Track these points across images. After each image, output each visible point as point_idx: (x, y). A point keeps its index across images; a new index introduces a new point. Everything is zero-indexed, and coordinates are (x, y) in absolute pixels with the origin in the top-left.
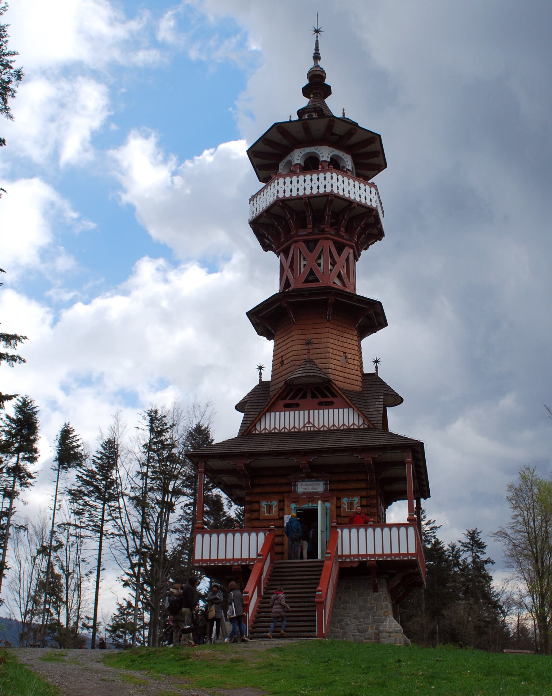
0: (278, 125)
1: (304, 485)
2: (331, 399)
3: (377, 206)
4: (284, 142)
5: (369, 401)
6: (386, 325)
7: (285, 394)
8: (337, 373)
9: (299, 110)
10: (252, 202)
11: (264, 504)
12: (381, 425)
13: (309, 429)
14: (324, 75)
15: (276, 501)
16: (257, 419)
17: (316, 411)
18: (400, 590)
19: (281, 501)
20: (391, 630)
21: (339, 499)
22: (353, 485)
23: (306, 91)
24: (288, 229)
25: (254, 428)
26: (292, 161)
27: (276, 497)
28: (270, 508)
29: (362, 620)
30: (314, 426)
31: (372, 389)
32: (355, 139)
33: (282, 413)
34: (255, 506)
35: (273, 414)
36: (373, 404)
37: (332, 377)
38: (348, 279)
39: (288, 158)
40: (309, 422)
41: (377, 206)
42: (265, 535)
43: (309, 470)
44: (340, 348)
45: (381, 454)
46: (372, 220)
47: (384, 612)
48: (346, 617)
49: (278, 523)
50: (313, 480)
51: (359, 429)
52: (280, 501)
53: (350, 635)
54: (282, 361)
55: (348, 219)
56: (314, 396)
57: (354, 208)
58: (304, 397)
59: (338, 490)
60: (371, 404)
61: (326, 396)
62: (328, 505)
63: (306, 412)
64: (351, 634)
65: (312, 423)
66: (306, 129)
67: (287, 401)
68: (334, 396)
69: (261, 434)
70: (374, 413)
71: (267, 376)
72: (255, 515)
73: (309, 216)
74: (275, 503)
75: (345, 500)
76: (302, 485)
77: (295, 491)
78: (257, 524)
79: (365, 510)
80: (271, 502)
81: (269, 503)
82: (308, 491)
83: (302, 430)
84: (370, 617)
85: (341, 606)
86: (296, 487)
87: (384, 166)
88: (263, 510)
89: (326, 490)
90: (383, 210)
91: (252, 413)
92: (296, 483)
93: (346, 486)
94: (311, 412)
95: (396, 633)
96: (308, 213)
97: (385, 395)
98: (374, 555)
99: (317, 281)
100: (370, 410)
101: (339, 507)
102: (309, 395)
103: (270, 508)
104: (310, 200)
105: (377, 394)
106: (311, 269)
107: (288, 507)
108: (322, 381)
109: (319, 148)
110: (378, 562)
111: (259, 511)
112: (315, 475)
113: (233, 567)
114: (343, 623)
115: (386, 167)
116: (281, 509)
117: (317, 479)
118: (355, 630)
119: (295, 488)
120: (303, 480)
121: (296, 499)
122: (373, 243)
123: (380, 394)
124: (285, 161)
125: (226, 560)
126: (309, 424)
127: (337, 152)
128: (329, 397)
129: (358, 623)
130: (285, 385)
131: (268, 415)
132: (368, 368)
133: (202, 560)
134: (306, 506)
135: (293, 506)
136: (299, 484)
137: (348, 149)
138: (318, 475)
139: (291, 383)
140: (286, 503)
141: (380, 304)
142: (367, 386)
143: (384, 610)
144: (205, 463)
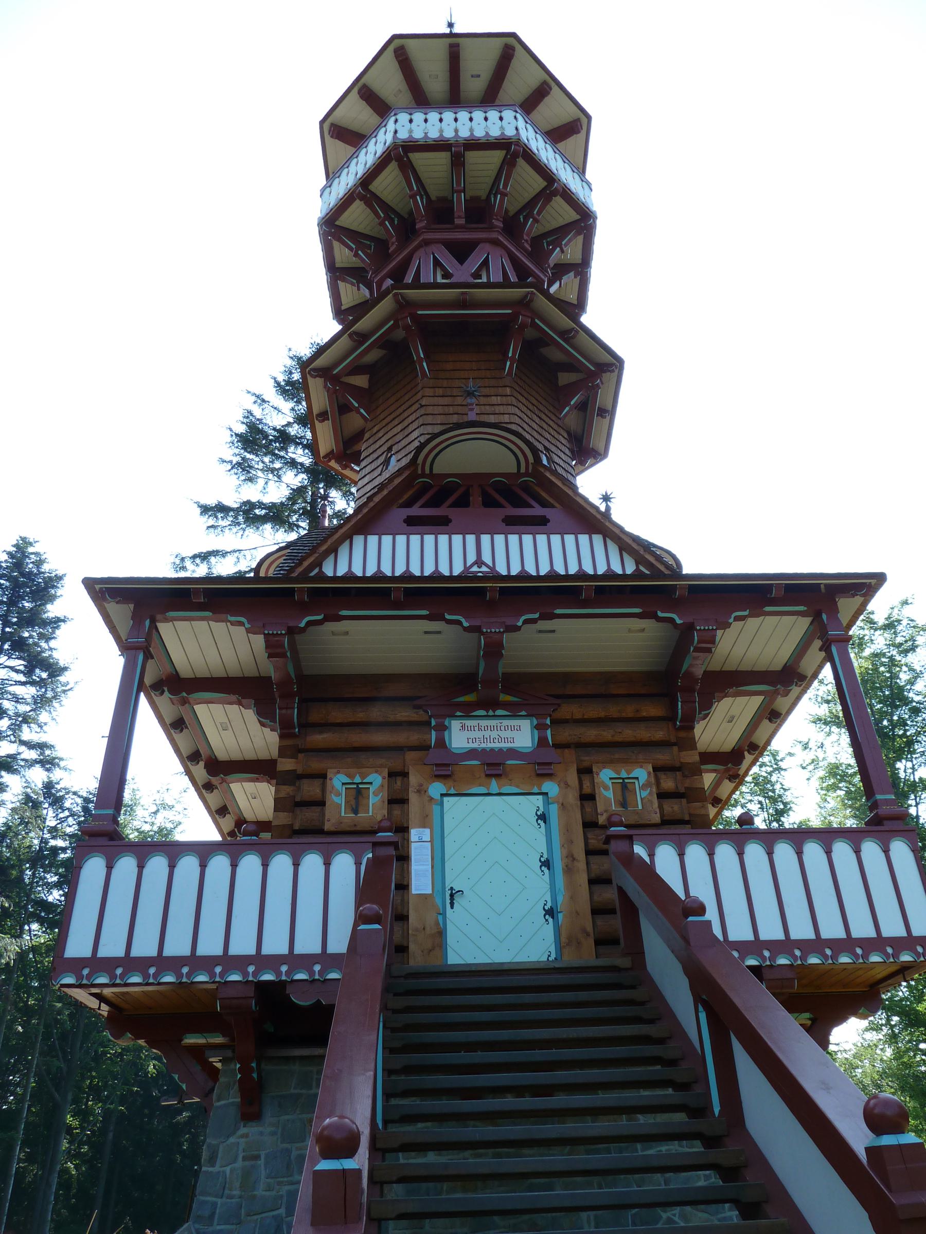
1: (470, 729)
11: (338, 781)
19: (397, 775)
21: (585, 771)
28: (358, 795)
33: (401, 539)
34: (310, 789)
35: (373, 540)
42: (358, 864)
50: (499, 712)
52: (392, 775)
58: (463, 502)
59: (581, 746)
62: (551, 788)
67: (416, 511)
72: (308, 815)
74: (376, 780)
75: (606, 775)
76: (463, 727)
79: (674, 808)
80: (363, 777)
82: (483, 746)
86: (446, 733)
88: (336, 799)
89: (542, 742)
93: (607, 734)
101: (588, 798)
103: (358, 795)
107: (419, 791)
111: (322, 803)
116: (397, 800)
117: (514, 711)
120: (467, 711)
131: (358, 540)
136: (455, 725)
139: (427, 471)
140: (414, 779)
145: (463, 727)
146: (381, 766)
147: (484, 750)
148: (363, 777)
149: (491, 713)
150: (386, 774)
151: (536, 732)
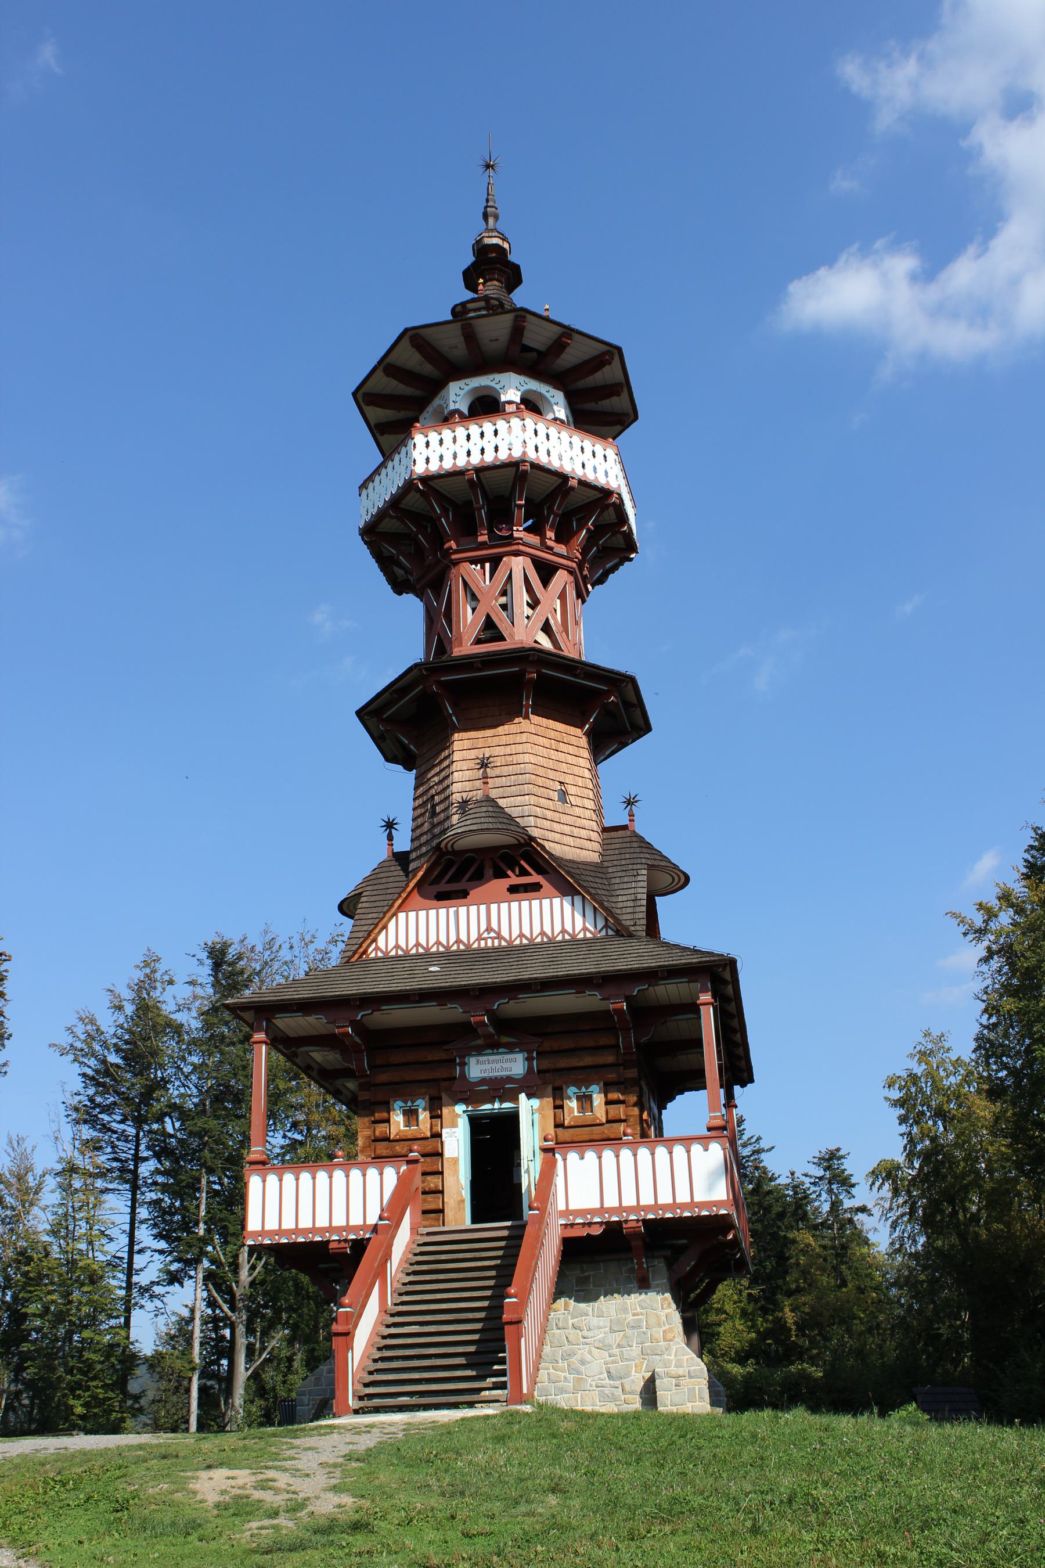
0: (410, 333)
1: (483, 1063)
2: (535, 878)
3: (619, 486)
4: (427, 369)
5: (617, 881)
6: (648, 729)
7: (436, 873)
8: (547, 824)
9: (456, 306)
10: (364, 492)
12: (644, 927)
13: (490, 944)
14: (506, 246)
15: (423, 1099)
16: (380, 926)
17: (504, 906)
18: (697, 1279)
20: (681, 1371)
22: (588, 1060)
23: (470, 278)
24: (438, 539)
25: (374, 946)
26: (445, 406)
27: (423, 1090)
29: (616, 1351)
30: (499, 936)
31: (623, 857)
32: (570, 357)
36: (625, 886)
37: (535, 833)
38: (564, 634)
39: (437, 402)
40: (489, 929)
41: (619, 486)
42: (398, 1173)
43: (491, 1030)
44: (551, 774)
45: (646, 986)
46: (610, 516)
47: (664, 1332)
48: (581, 1346)
49: (430, 1146)
51: (594, 940)
53: (591, 1385)
54: (434, 807)
55: (560, 512)
56: (501, 874)
57: (572, 488)
60: (621, 886)
61: (524, 873)
63: (483, 908)
64: (594, 1383)
65: (495, 932)
66: (470, 336)
67: (443, 887)
68: (540, 871)
69: (386, 958)
70: (630, 904)
71: (403, 843)
73: (479, 510)
77: (463, 1074)
78: (382, 1148)
80: (413, 1102)
81: (409, 1104)
82: (491, 1074)
83: (476, 945)
84: (635, 1345)
85: (570, 1322)
86: (466, 1067)
87: (632, 417)
89: (530, 1069)
90: (633, 499)
91: (370, 916)
92: (466, 1060)
93: (575, 1062)
94: (494, 907)
95: (690, 1377)
96: (478, 502)
97: (651, 867)
98: (638, 1208)
99: (501, 638)
100: (620, 899)
102: (489, 872)
104: (481, 474)
105: (635, 867)
106: (488, 616)
108: (516, 842)
109: (498, 377)
110: (646, 1222)
112: (505, 1039)
113: (332, 1246)
114: (573, 1359)
115: (636, 418)
117: (511, 1048)
118: (601, 1373)
119: (463, 1073)
120: (479, 1051)
121: (469, 1093)
122: (614, 569)
123: (639, 866)
124: (430, 409)
125: (314, 1230)
126: (489, 933)
127: (533, 385)
128: (531, 875)
129: (609, 1359)
130: (437, 853)
131: (402, 916)
132: (617, 817)
133: (263, 1233)
134: (488, 1106)
135: (460, 1108)
136: (473, 1061)
137: (557, 380)
138: (512, 1040)
141: (632, 680)
142: (612, 852)
143: (664, 1328)
144: (269, 1021)
145: (478, 1062)
146: (425, 1094)
147: (491, 1079)
148: (413, 1102)
149: (495, 1051)
150: (427, 1098)
151: (526, 1062)
